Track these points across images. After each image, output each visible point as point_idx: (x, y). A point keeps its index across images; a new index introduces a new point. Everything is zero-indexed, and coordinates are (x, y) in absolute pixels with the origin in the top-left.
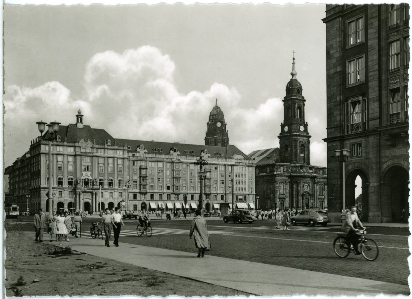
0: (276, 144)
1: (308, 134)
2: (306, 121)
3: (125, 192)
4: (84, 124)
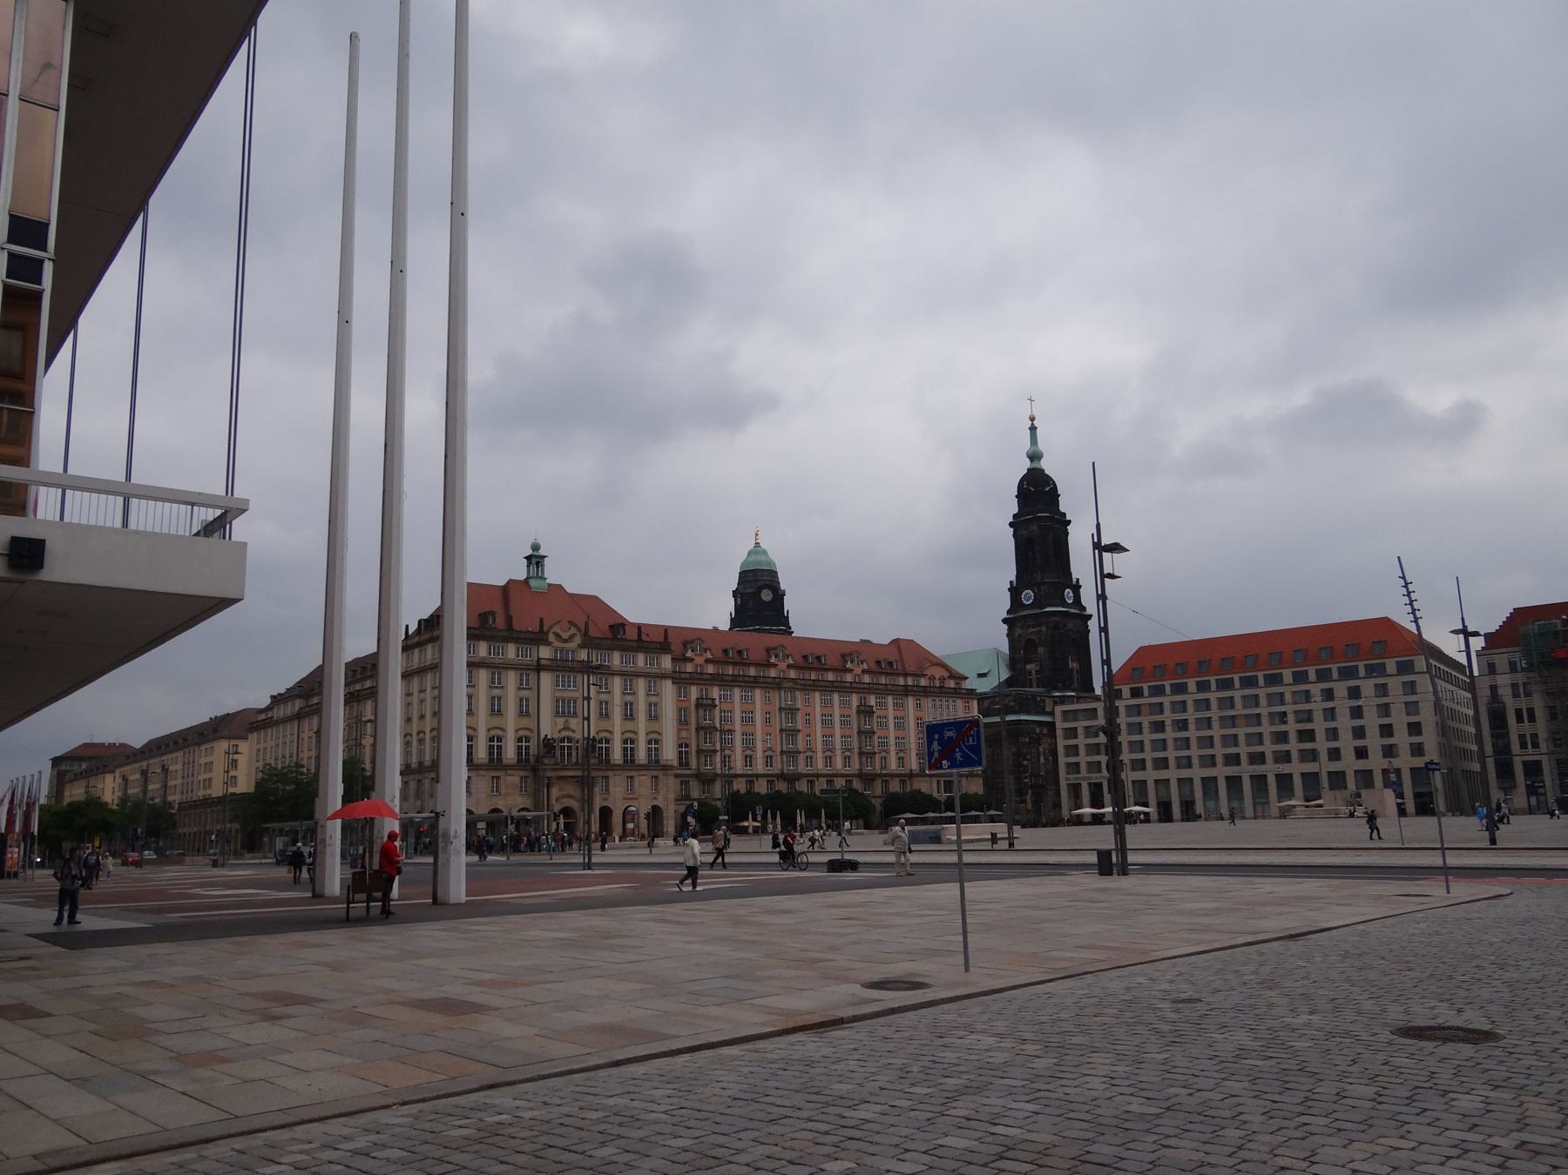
0: (1000, 639)
1: (1084, 609)
2: (1074, 576)
3: (667, 775)
4: (548, 581)
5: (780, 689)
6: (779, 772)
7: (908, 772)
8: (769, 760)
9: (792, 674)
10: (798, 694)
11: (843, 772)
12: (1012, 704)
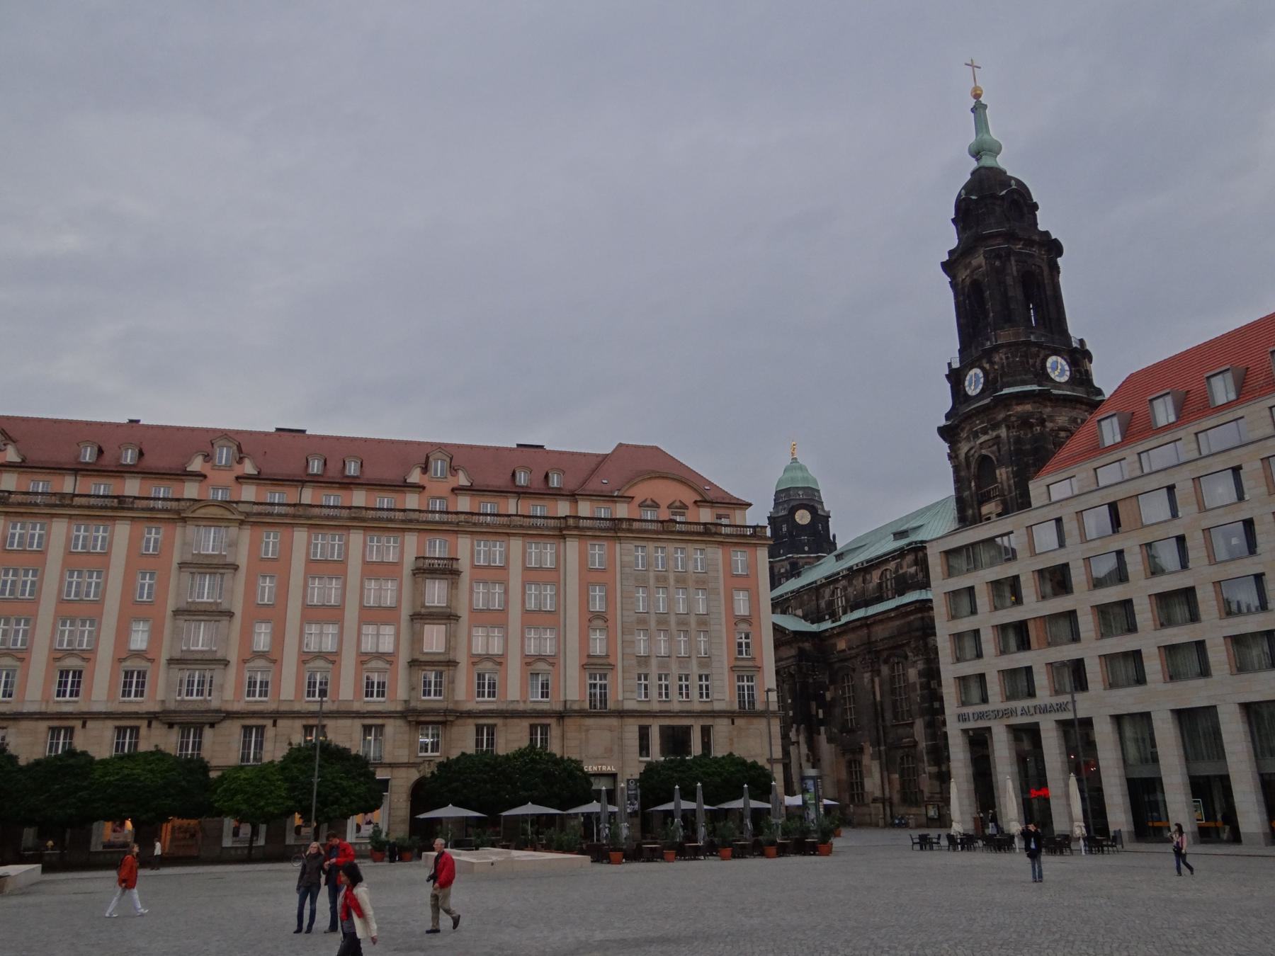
5: (184, 520)
6: (157, 708)
7: (558, 707)
8: (133, 681)
9: (249, 493)
10: (245, 536)
11: (356, 706)
12: (913, 570)
